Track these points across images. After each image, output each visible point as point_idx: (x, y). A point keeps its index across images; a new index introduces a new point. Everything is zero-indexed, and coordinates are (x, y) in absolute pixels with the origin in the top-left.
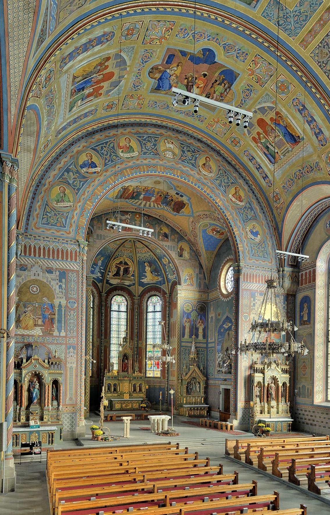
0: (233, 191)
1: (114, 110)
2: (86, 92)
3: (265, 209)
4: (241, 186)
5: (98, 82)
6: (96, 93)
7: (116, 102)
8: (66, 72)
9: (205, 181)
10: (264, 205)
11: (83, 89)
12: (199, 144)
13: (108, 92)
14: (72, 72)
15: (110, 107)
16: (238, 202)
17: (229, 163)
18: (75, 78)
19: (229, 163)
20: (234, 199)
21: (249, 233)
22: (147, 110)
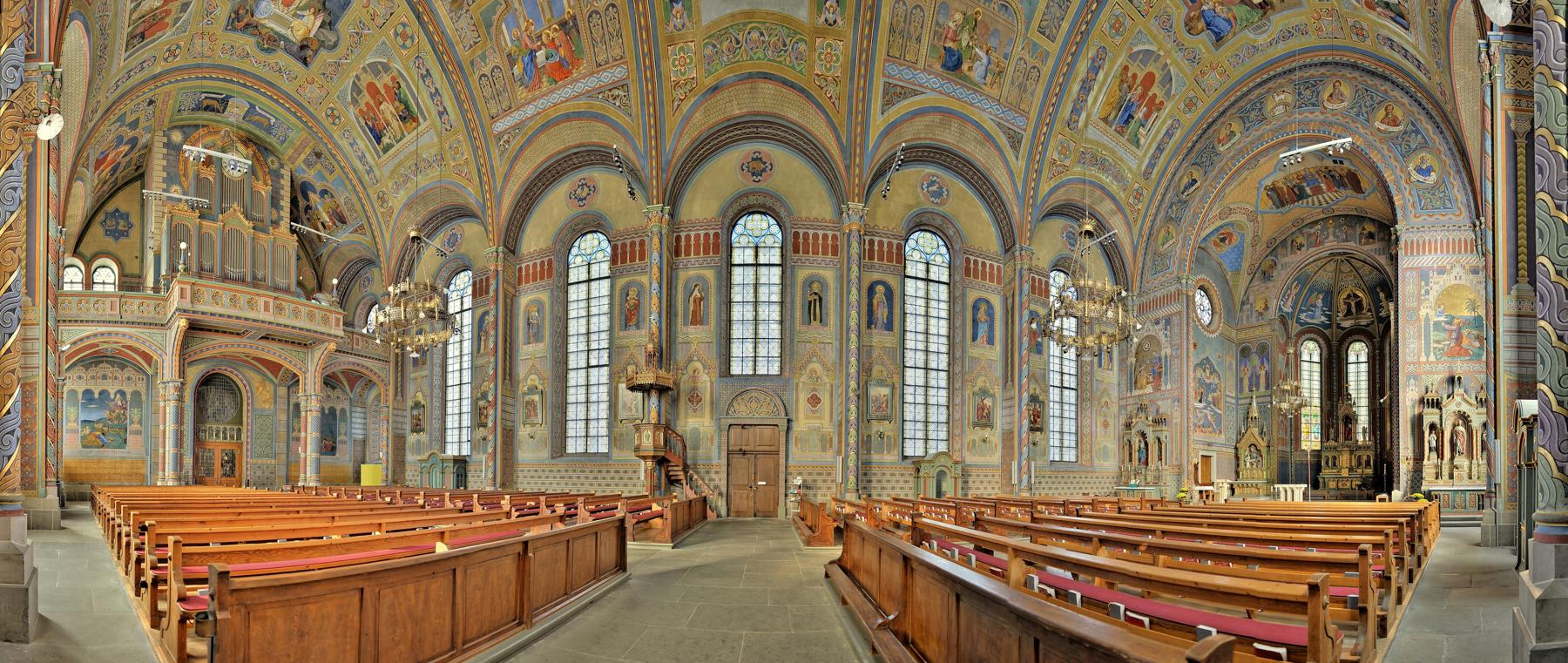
0: (1382, 113)
1: (1200, 104)
2: (1140, 115)
3: (1443, 126)
4: (1396, 101)
5: (1143, 96)
6: (1154, 106)
7: (1191, 94)
8: (1086, 126)
9: (1333, 119)
10: (1438, 119)
11: (1131, 117)
12: (1322, 70)
13: (1168, 93)
14: (1095, 117)
15: (1190, 105)
16: (1391, 129)
17: (1373, 74)
18: (1105, 120)
19: (1373, 74)
20: (1383, 127)
21: (1414, 173)
22: (1238, 73)
